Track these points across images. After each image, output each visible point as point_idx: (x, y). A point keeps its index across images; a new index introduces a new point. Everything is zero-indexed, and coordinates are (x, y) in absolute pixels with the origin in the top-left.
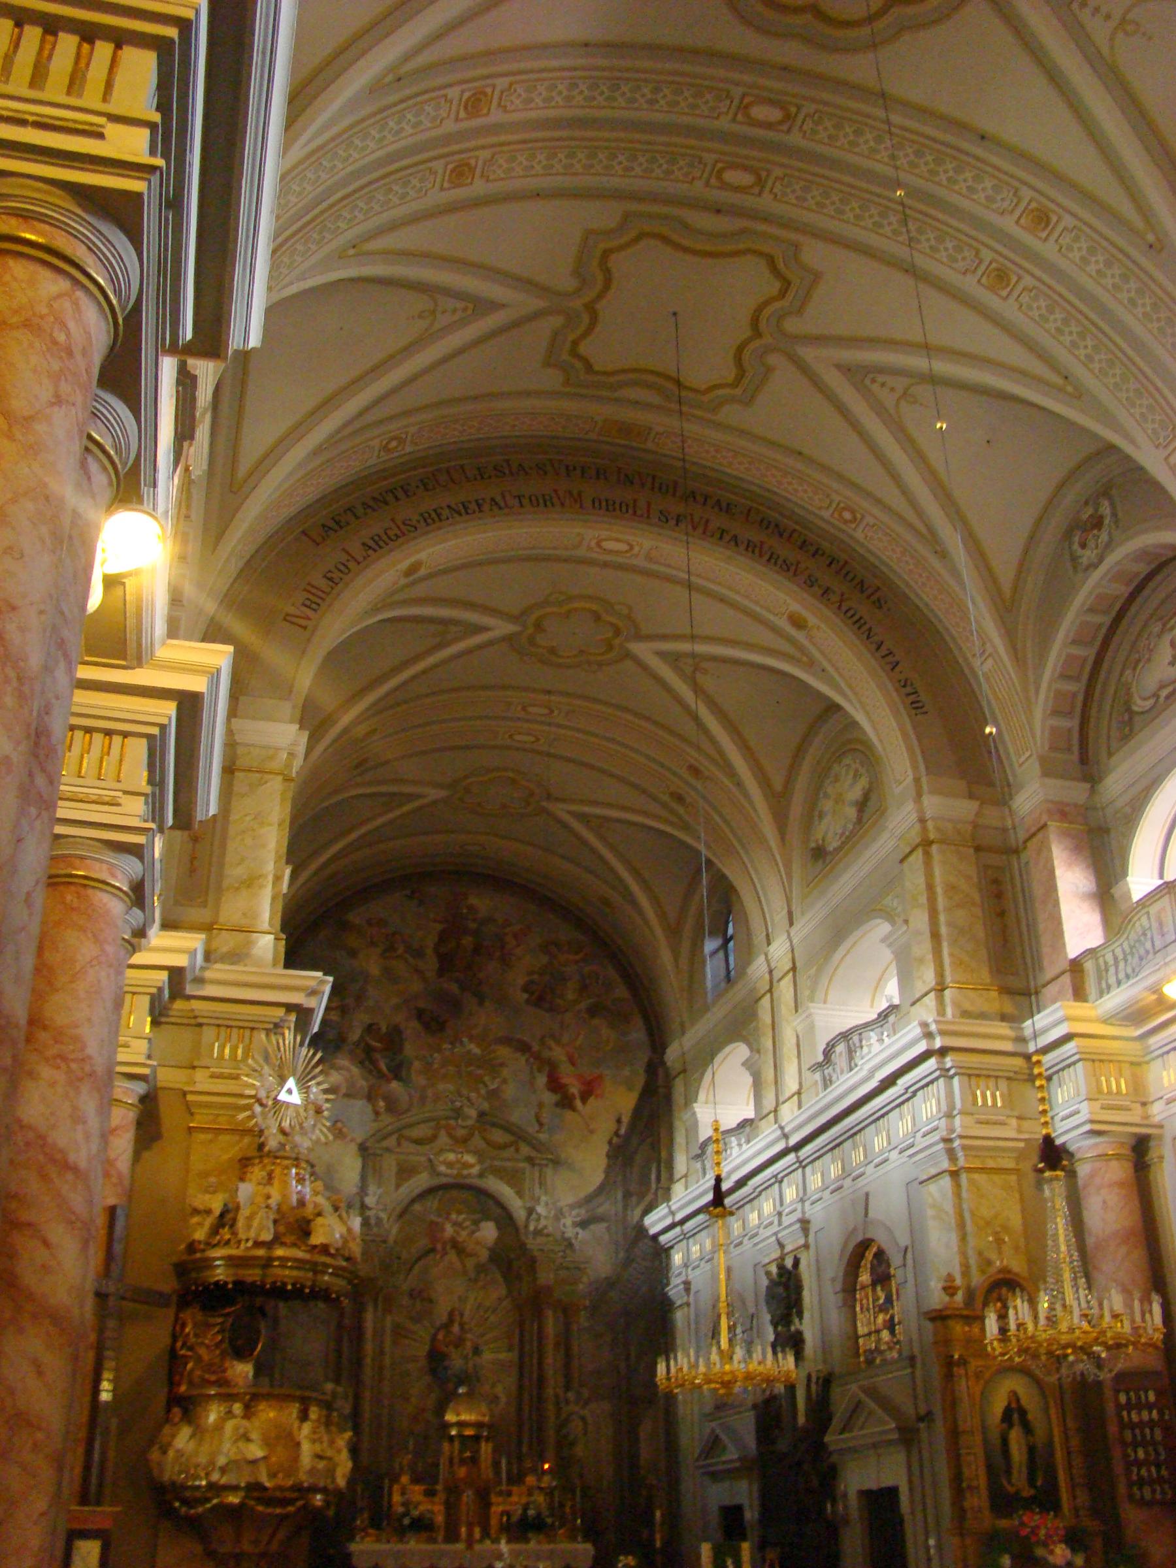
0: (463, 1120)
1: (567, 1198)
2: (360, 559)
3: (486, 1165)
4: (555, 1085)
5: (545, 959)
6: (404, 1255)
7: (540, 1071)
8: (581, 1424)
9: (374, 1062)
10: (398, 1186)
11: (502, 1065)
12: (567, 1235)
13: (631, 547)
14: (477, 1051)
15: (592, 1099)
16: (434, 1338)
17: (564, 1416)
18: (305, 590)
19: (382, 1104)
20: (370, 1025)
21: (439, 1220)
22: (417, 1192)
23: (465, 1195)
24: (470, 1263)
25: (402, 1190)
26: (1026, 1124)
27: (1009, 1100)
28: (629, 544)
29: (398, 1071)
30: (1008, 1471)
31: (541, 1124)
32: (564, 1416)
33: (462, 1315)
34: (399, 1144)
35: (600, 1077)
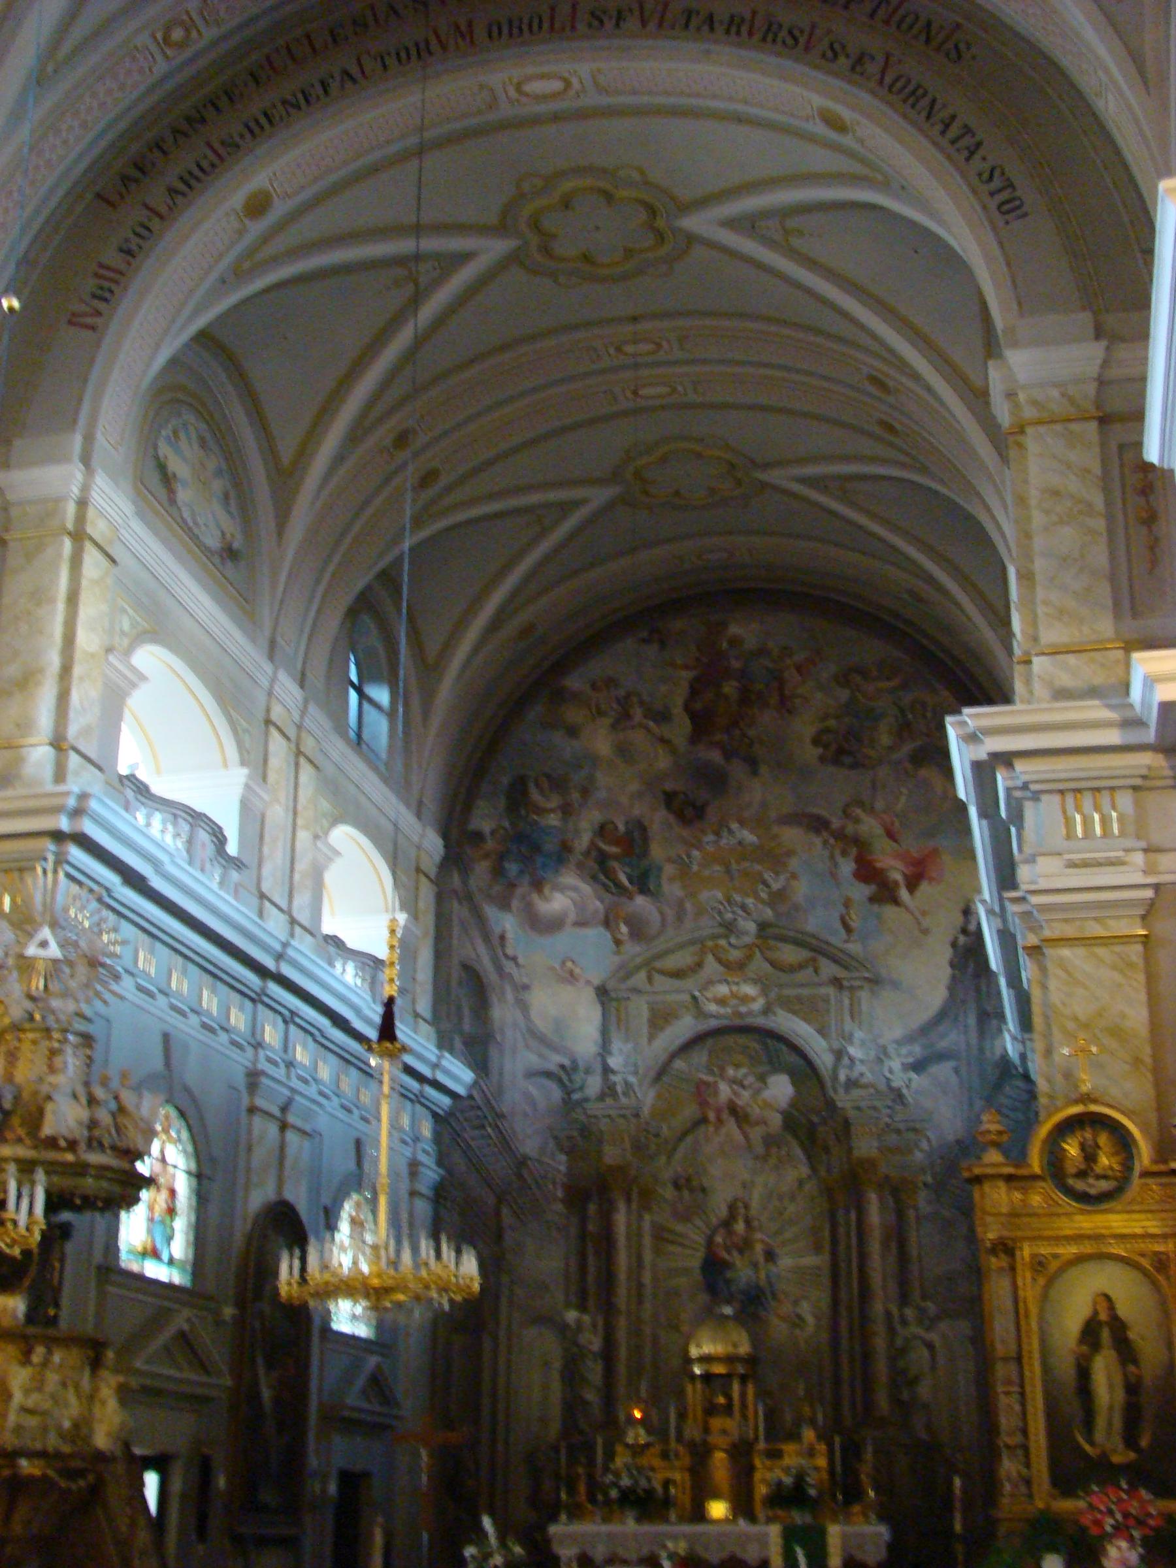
0: (738, 937)
2: (163, 209)
3: (773, 995)
4: (867, 872)
5: (844, 695)
6: (665, 1131)
7: (844, 853)
8: (925, 1353)
9: (609, 874)
10: (651, 1038)
11: (790, 853)
12: (895, 1084)
13: (568, 84)
15: (924, 887)
16: (710, 1242)
17: (899, 1342)
19: (624, 929)
21: (710, 1079)
22: (678, 1043)
23: (743, 1040)
24: (756, 1133)
27: (1138, 826)
28: (561, 78)
29: (644, 883)
30: (1088, 1424)
31: (848, 929)
32: (899, 1342)
33: (747, 1207)
34: (650, 979)
35: (935, 852)
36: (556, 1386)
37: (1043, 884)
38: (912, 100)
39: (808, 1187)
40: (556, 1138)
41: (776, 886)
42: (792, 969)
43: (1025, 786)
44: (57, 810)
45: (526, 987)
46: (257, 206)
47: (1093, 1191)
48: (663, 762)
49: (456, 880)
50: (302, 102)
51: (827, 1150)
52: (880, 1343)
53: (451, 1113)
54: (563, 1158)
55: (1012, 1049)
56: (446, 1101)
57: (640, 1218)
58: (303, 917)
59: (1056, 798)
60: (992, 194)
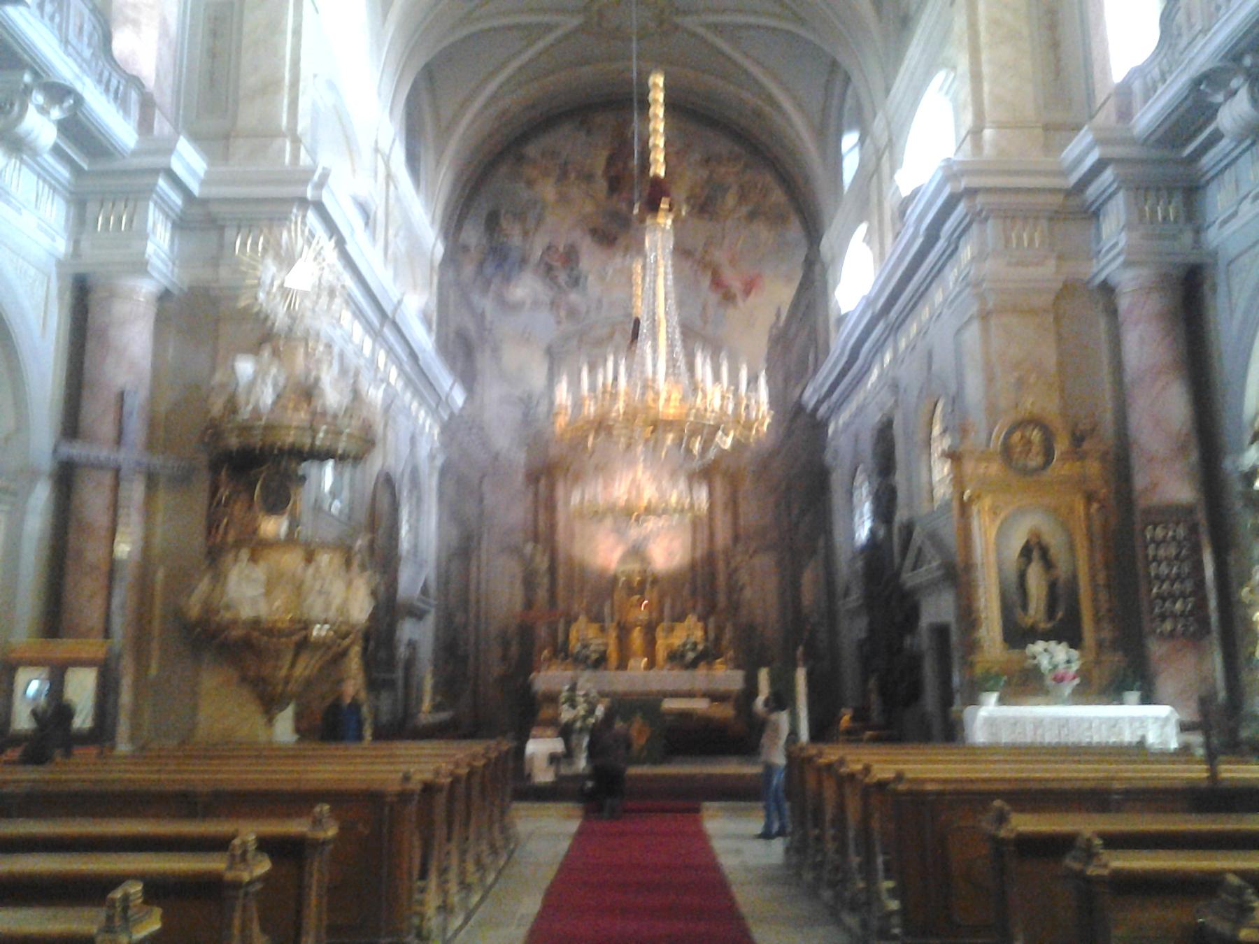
4: (717, 283)
5: (704, 173)
17: (733, 565)
30: (1025, 607)
35: (759, 276)
48: (589, 208)
49: (451, 275)
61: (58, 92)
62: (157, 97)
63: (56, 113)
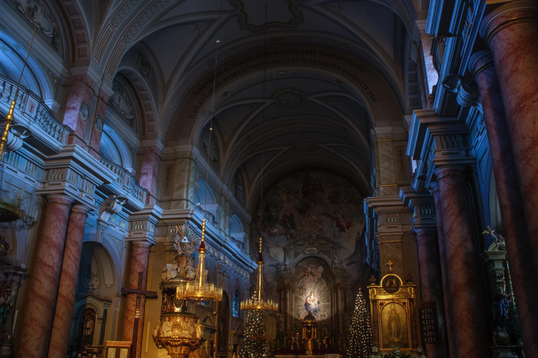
1: (344, 257)
4: (339, 225)
10: (294, 259)
12: (344, 268)
14: (315, 218)
15: (350, 228)
17: (344, 320)
18: (194, 108)
19: (289, 236)
20: (284, 215)
21: (307, 267)
22: (300, 259)
24: (316, 278)
25: (296, 259)
26: (405, 227)
29: (293, 227)
31: (335, 237)
32: (344, 320)
36: (275, 328)
37: (383, 231)
38: (354, 79)
39: (326, 289)
40: (275, 278)
41: (320, 228)
42: (323, 245)
43: (379, 212)
44: (188, 213)
45: (269, 248)
46: (225, 94)
47: (392, 290)
50: (235, 75)
51: (330, 281)
52: (341, 320)
53: (253, 273)
54: (276, 282)
55: (368, 261)
56: (252, 271)
57: (292, 295)
58: (227, 233)
59: (385, 214)
60: (370, 97)
61: (122, 199)
62: (151, 193)
63: (122, 203)
